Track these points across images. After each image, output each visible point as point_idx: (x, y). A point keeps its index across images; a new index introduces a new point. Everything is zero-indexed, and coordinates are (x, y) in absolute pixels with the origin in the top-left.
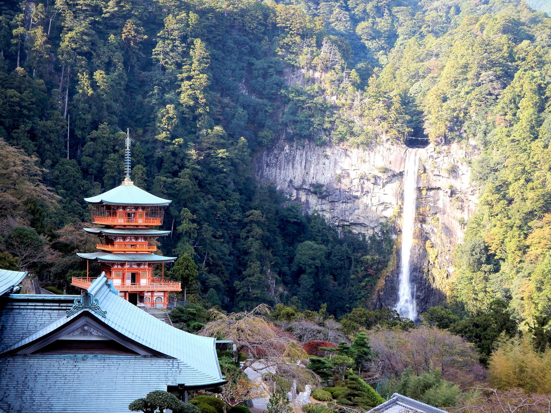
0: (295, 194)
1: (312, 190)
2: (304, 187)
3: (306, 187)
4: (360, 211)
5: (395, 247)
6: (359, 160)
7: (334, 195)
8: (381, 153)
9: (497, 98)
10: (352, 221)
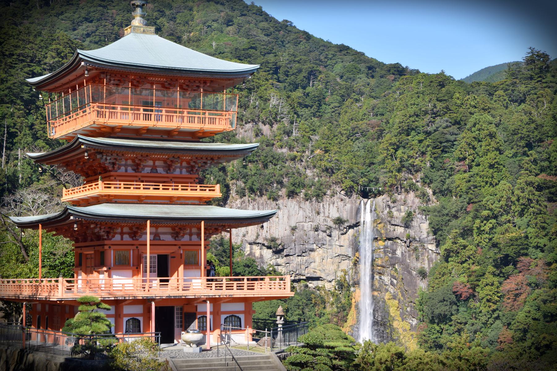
0: (248, 248)
1: (266, 244)
2: (258, 241)
3: (260, 240)
4: (317, 264)
5: (353, 300)
6: (314, 212)
7: (289, 248)
8: (336, 205)
9: (454, 145)
10: (309, 275)
